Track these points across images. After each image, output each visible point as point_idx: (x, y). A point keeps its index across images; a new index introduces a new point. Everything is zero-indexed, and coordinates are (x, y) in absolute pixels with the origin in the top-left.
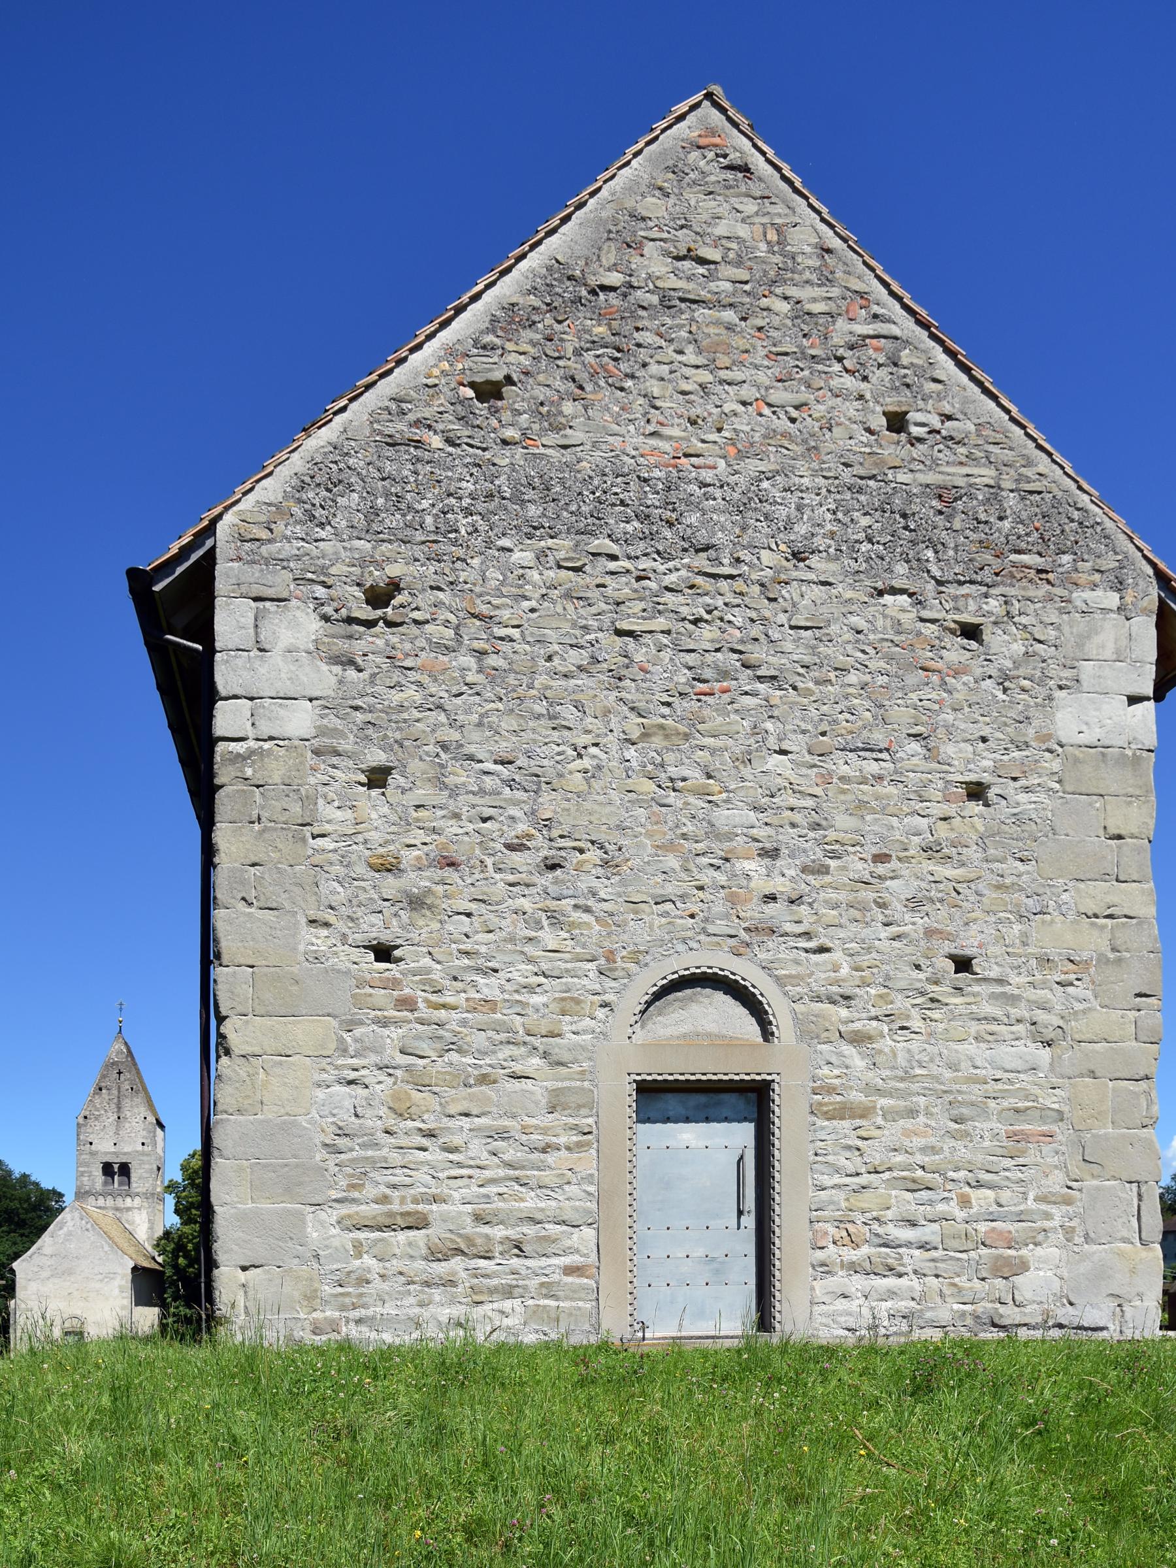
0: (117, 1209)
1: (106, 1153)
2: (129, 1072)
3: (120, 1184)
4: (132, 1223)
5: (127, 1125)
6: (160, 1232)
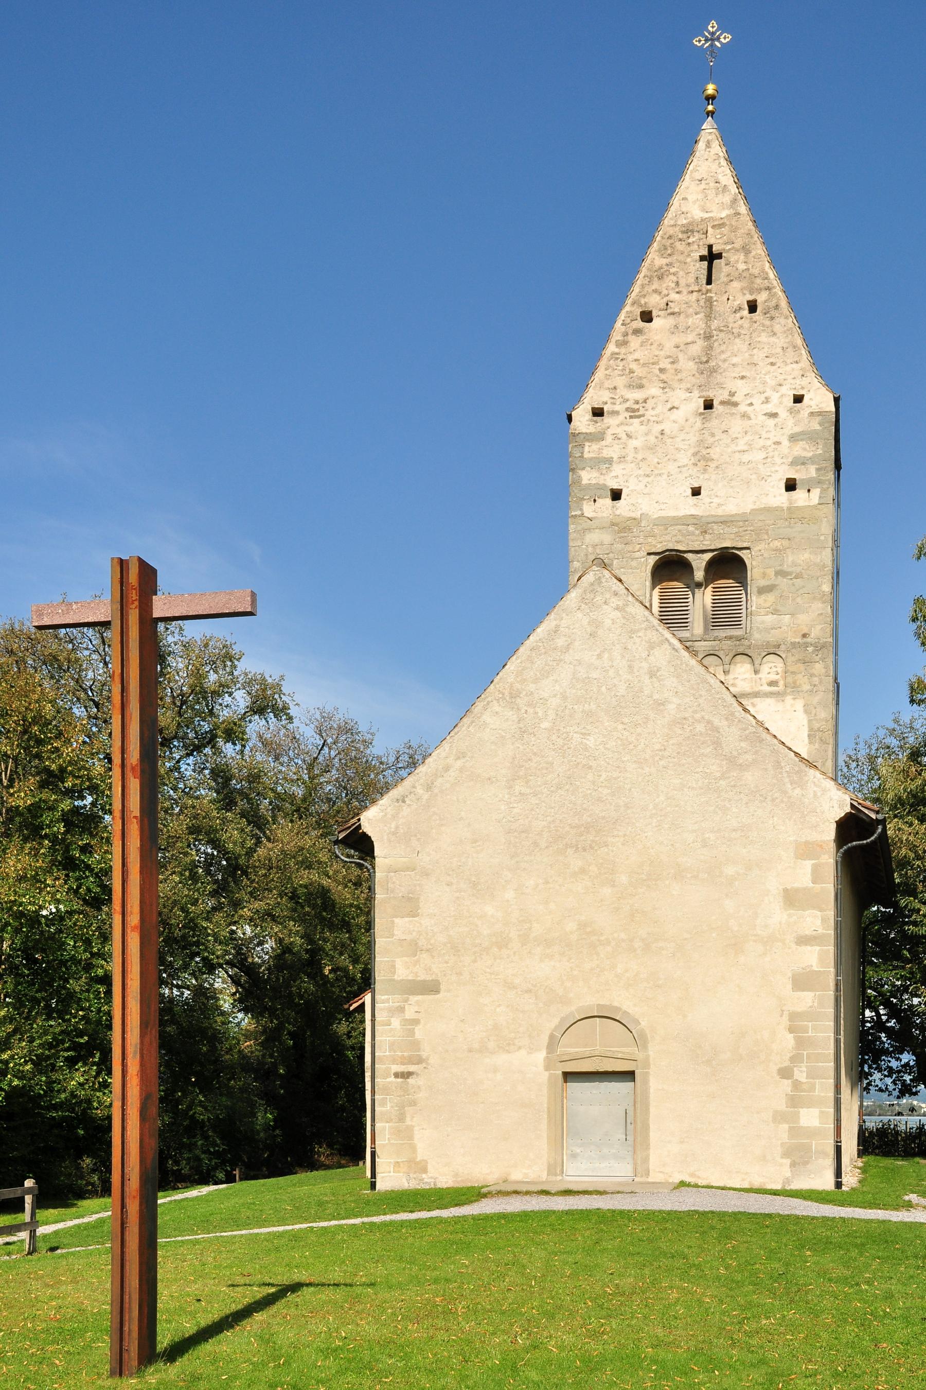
1: (666, 523)
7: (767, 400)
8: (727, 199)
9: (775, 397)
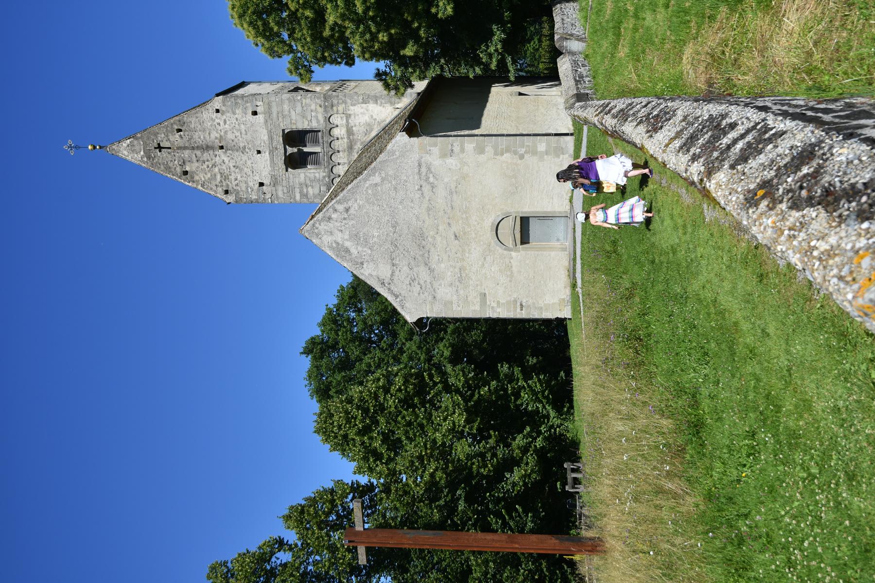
0: (350, 148)
2: (156, 134)
3: (316, 142)
4: (369, 126)
5: (230, 136)
6: (378, 85)
7: (219, 124)
8: (136, 142)
9: (217, 121)
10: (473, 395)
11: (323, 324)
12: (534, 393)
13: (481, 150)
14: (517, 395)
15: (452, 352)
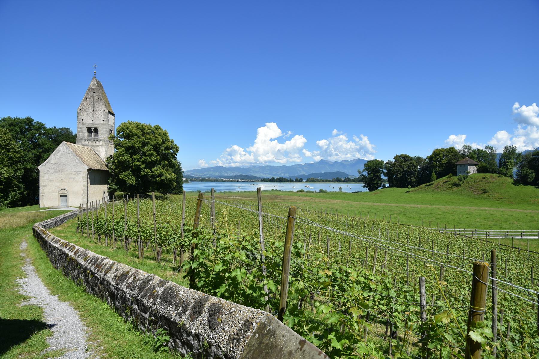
0: (93, 146)
3: (95, 136)
4: (99, 151)
5: (97, 113)
10: (14, 178)
11: (38, 123)
12: (15, 196)
13: (84, 186)
14: (13, 191)
15: (28, 169)
